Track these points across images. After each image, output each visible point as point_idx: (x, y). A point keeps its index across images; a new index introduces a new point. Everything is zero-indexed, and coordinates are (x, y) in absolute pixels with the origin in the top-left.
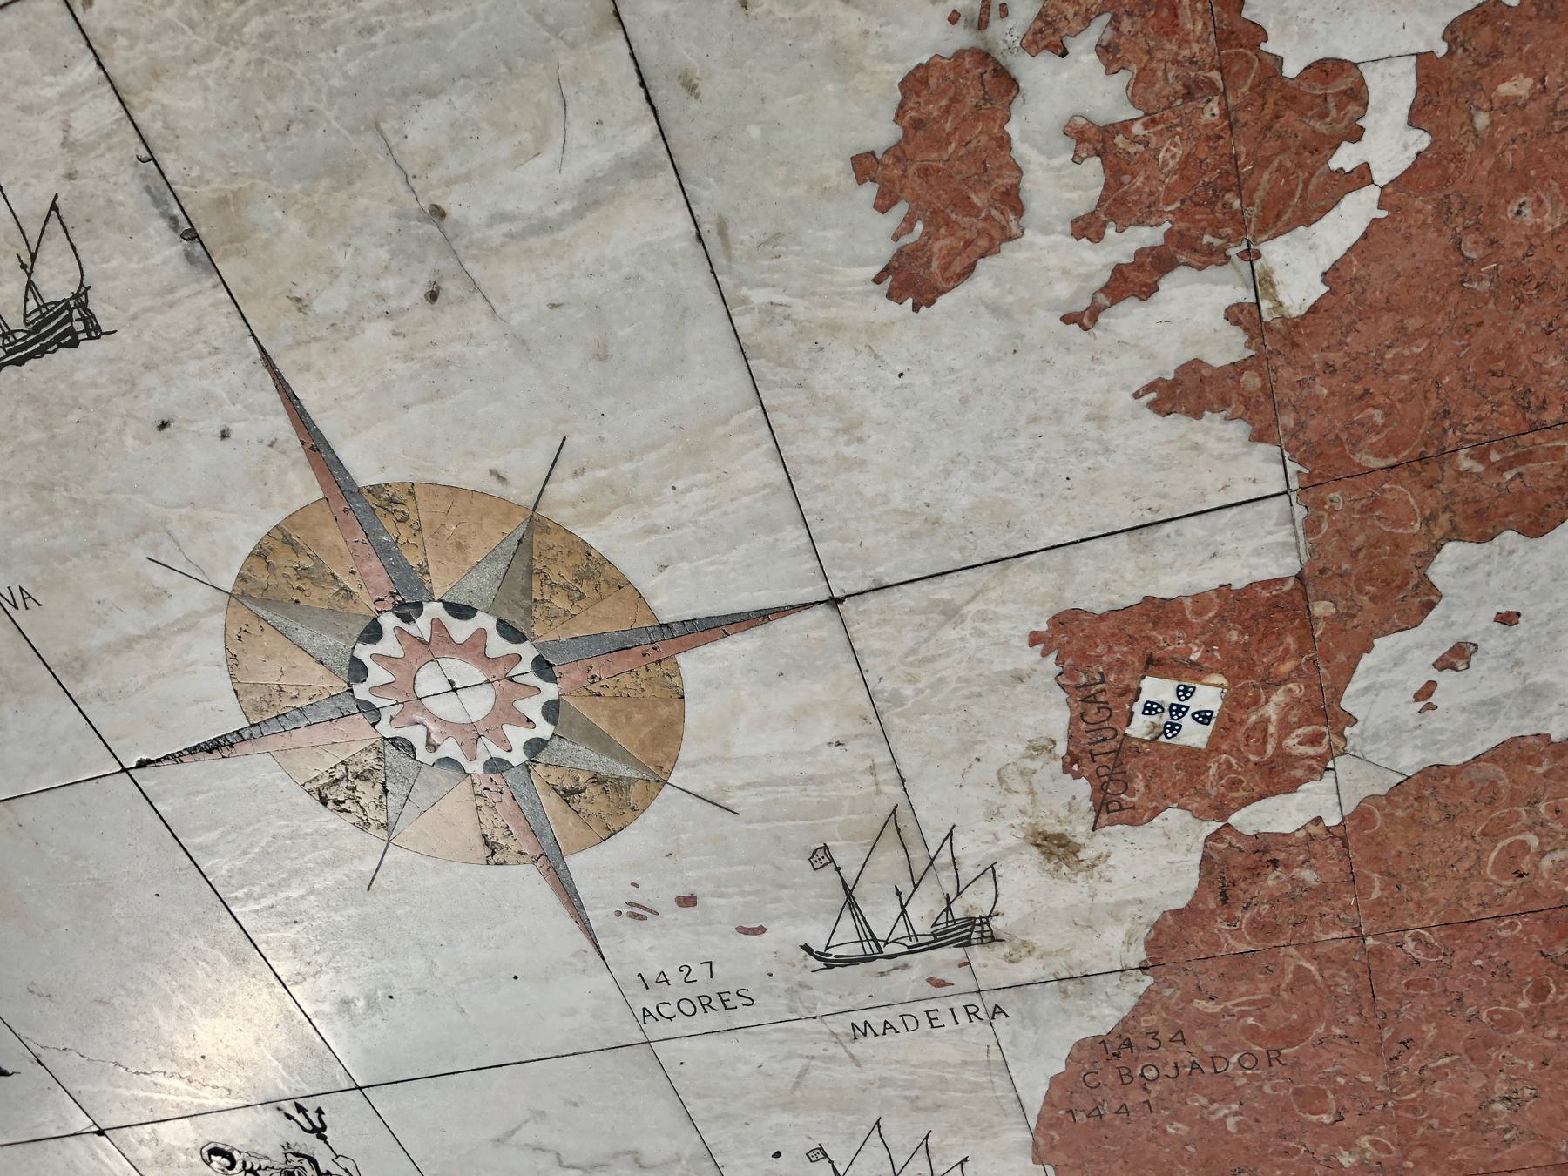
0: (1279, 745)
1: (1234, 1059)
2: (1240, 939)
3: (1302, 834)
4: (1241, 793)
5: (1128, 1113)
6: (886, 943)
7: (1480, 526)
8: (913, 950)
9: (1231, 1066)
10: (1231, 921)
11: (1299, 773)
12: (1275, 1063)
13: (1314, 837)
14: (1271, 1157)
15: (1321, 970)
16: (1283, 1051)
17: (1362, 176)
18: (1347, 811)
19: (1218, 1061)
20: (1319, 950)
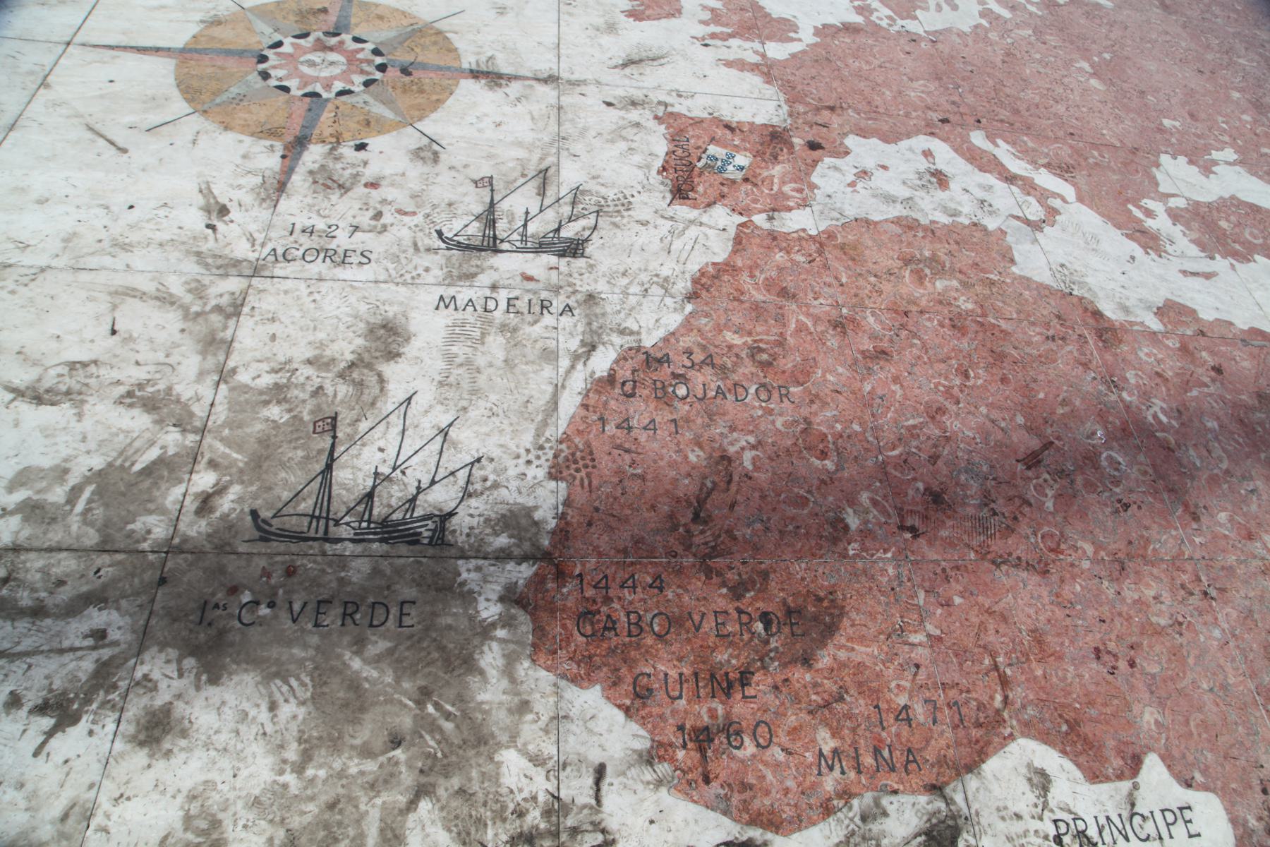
0: (780, 189)
1: (752, 390)
2: (758, 289)
3: (795, 235)
4: (758, 206)
5: (655, 430)
6: (502, 241)
7: (863, 133)
8: (518, 251)
9: (750, 397)
10: (752, 276)
11: (791, 204)
12: (785, 400)
13: (802, 238)
14: (783, 506)
15: (815, 325)
16: (792, 389)
17: (800, 40)
18: (821, 229)
19: (740, 390)
20: (812, 310)
